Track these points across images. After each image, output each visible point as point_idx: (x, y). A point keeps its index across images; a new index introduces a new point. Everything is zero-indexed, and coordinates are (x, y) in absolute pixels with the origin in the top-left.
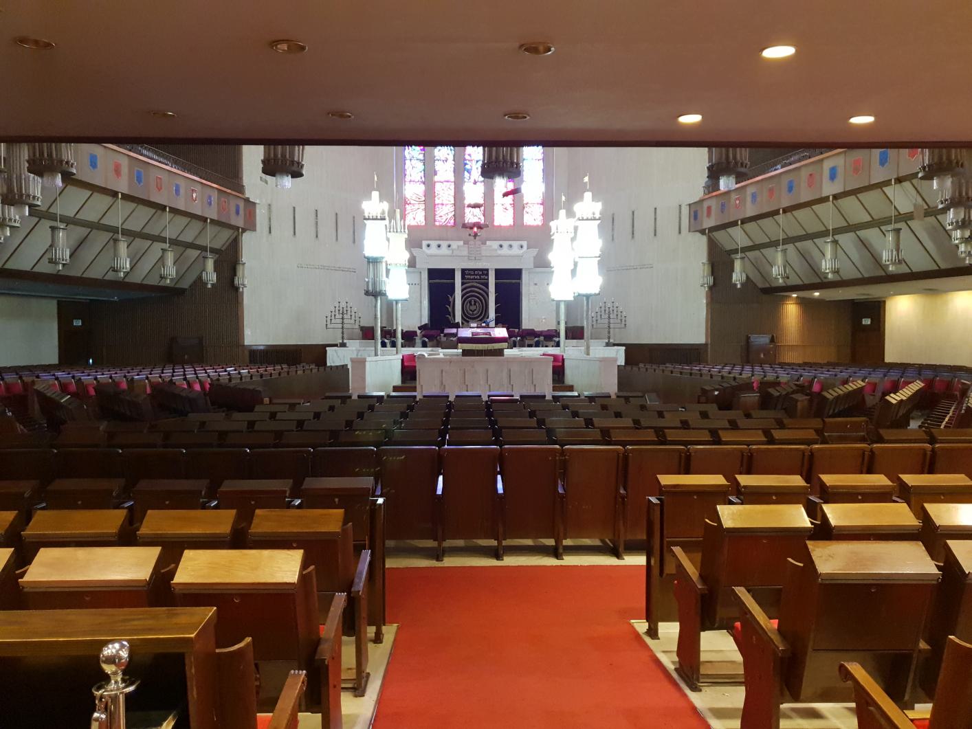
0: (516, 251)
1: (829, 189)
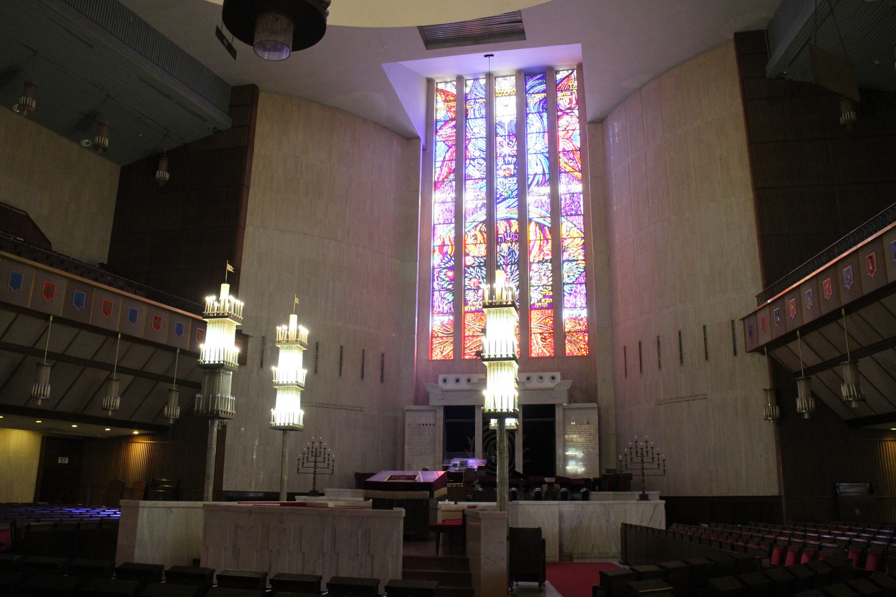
0: (547, 383)
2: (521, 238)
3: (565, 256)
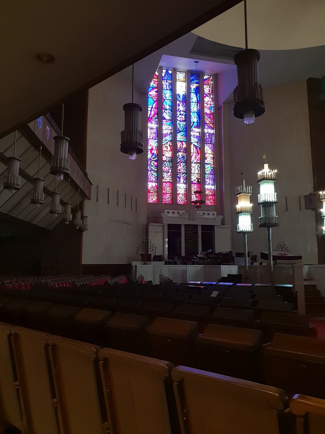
0: (211, 216)
2: (187, 151)
3: (206, 161)
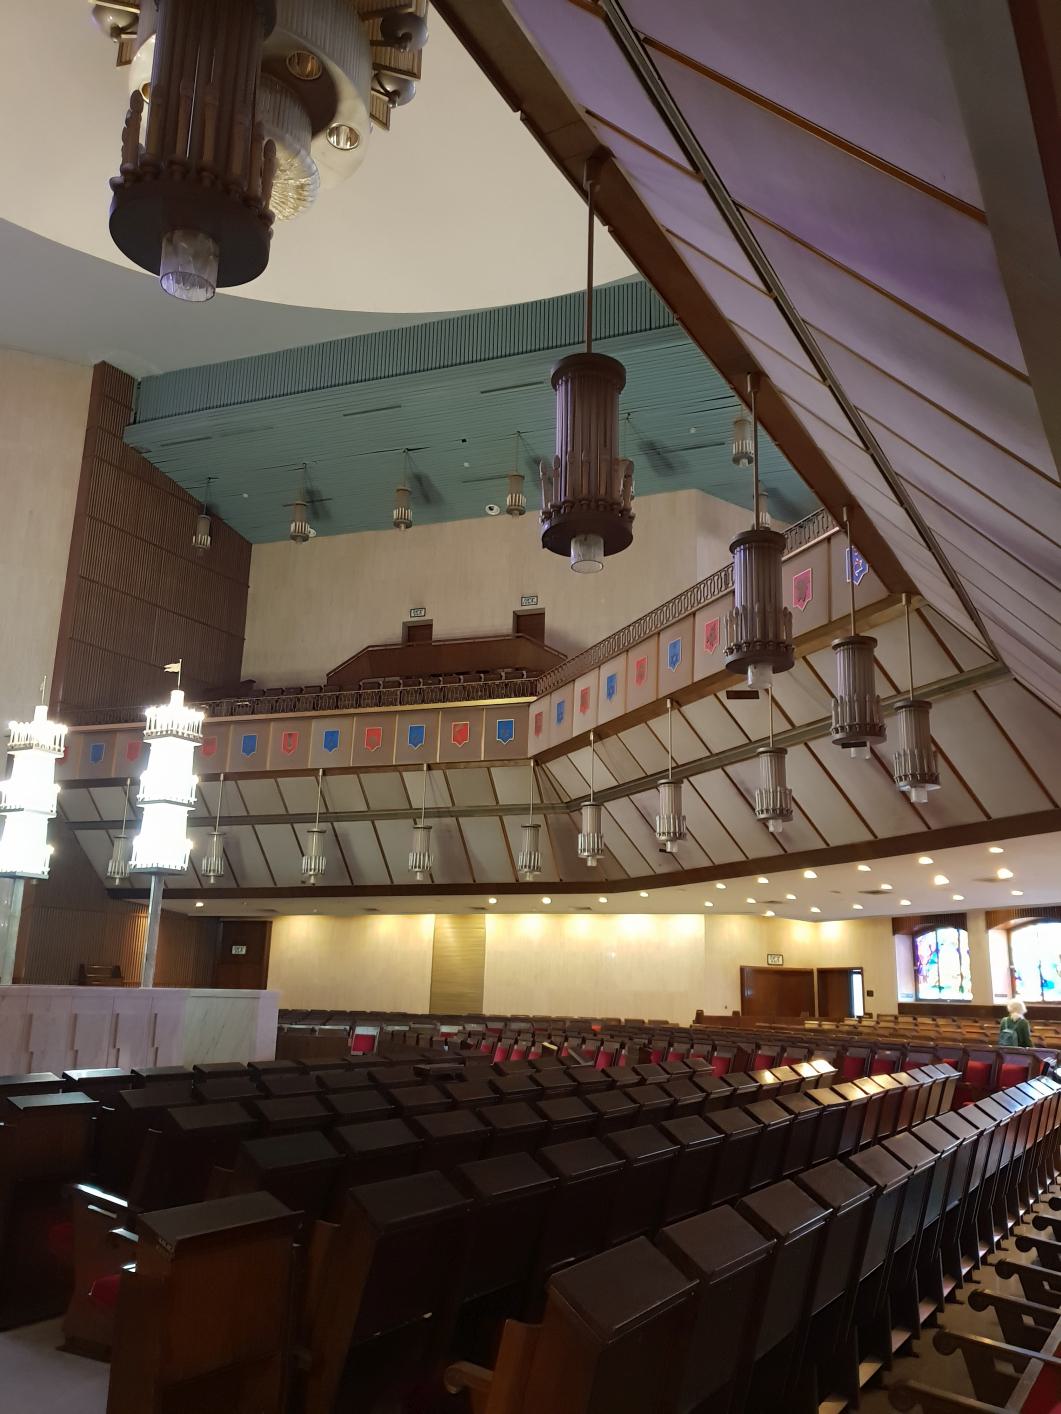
1: (317, 756)
